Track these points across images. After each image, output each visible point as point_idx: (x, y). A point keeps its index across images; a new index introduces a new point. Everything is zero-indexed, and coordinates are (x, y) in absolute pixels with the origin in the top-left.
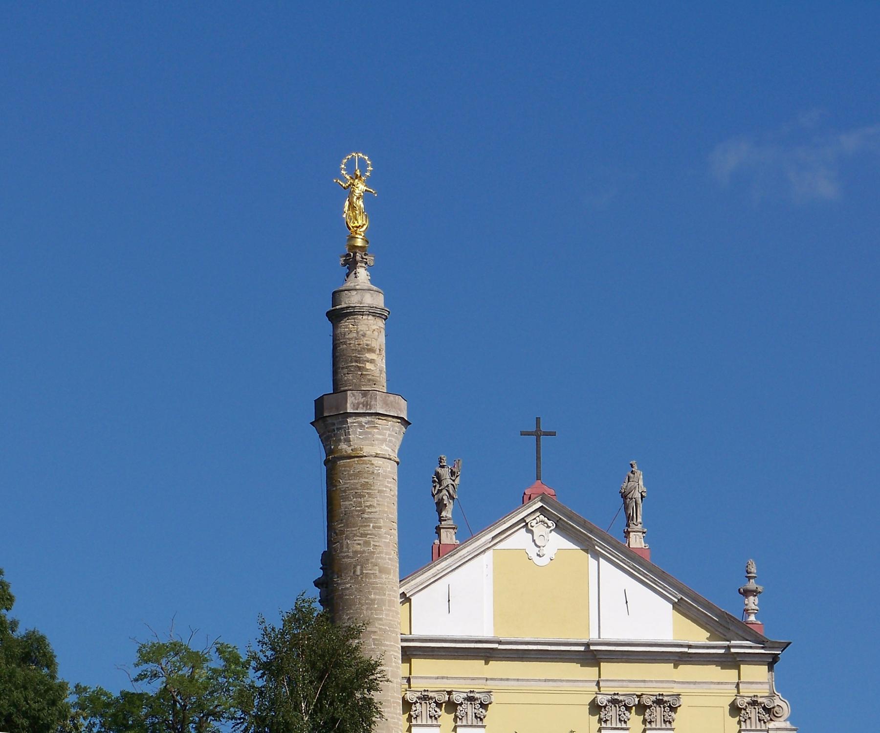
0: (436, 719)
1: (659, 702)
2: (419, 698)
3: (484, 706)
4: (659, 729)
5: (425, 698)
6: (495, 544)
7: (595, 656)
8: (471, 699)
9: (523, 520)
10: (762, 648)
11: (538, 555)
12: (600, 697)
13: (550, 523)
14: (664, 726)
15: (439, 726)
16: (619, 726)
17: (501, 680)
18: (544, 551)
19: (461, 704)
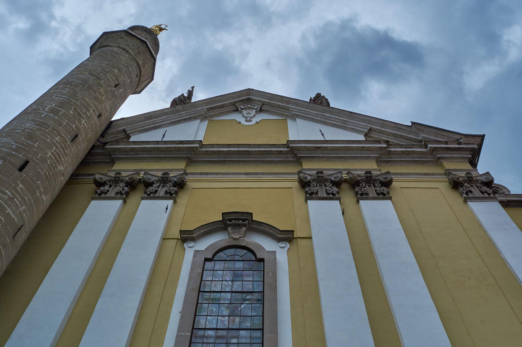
0: (122, 194)
1: (369, 179)
2: (110, 181)
3: (175, 184)
4: (374, 198)
5: (117, 180)
6: (212, 116)
7: (296, 155)
8: (164, 180)
9: (234, 104)
10: (459, 143)
11: (246, 121)
12: (302, 175)
13: (256, 107)
14: (376, 196)
15: (125, 202)
16: (325, 196)
17: (201, 174)
18: (253, 119)
19: (151, 184)
